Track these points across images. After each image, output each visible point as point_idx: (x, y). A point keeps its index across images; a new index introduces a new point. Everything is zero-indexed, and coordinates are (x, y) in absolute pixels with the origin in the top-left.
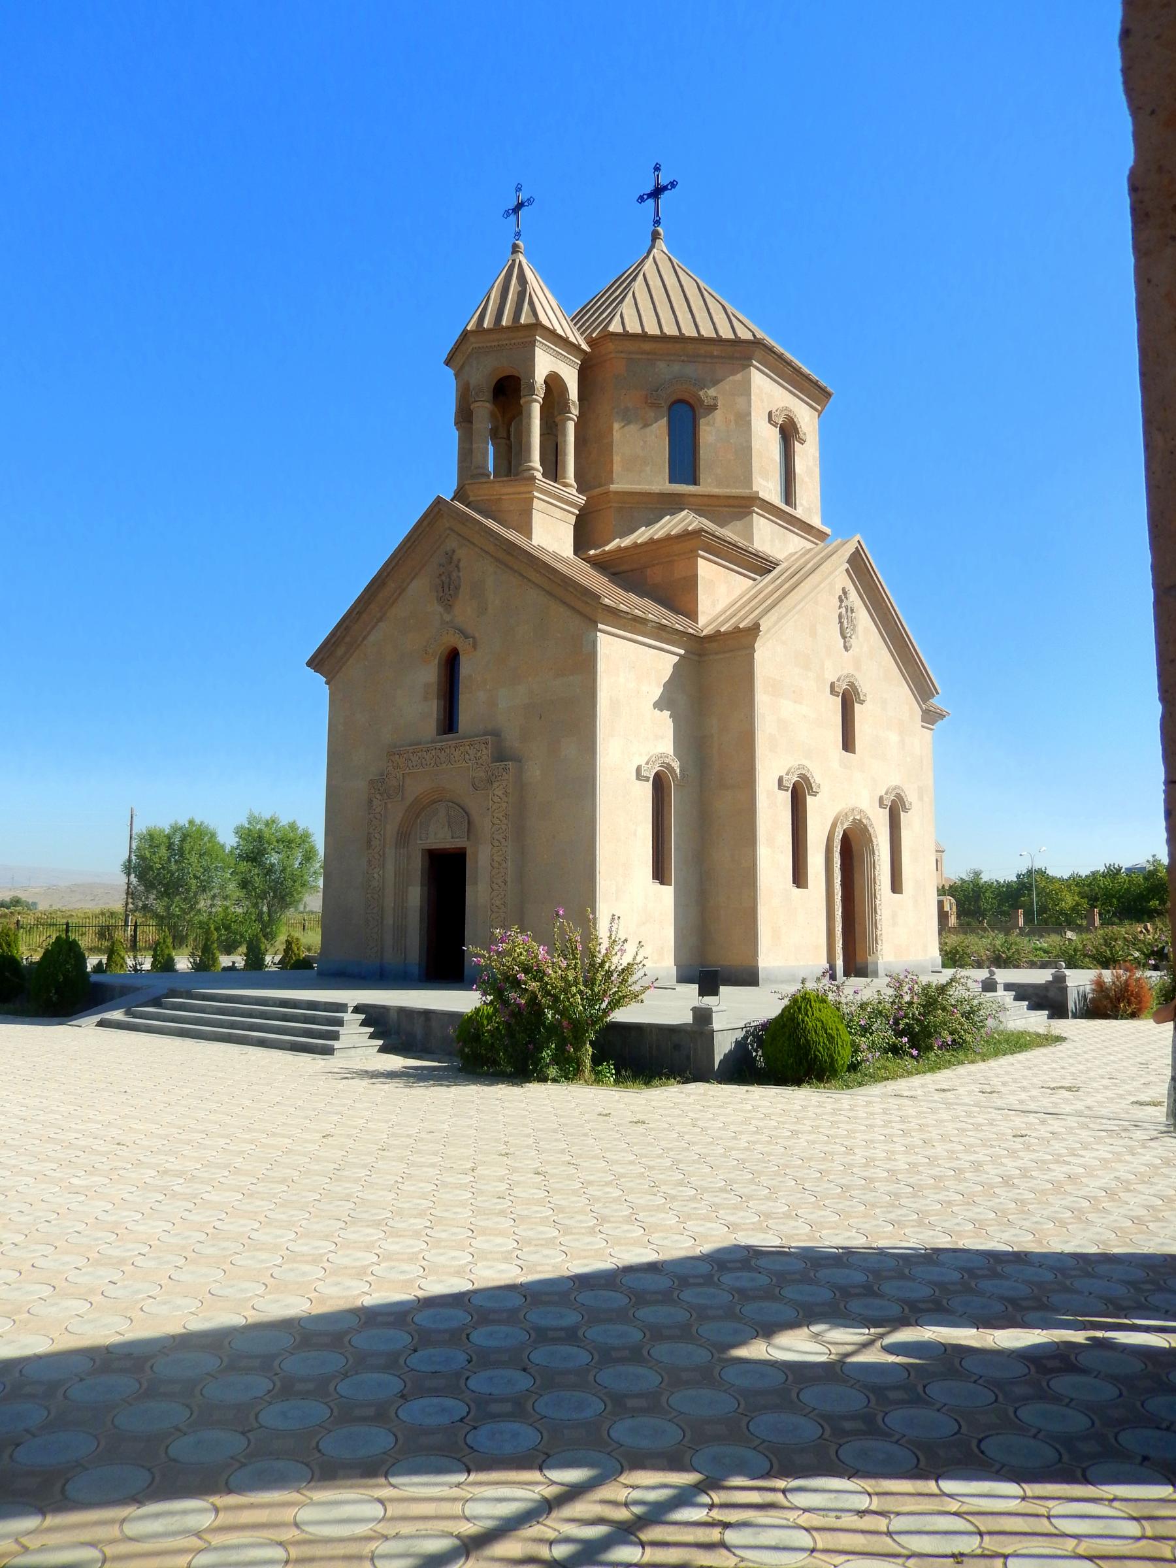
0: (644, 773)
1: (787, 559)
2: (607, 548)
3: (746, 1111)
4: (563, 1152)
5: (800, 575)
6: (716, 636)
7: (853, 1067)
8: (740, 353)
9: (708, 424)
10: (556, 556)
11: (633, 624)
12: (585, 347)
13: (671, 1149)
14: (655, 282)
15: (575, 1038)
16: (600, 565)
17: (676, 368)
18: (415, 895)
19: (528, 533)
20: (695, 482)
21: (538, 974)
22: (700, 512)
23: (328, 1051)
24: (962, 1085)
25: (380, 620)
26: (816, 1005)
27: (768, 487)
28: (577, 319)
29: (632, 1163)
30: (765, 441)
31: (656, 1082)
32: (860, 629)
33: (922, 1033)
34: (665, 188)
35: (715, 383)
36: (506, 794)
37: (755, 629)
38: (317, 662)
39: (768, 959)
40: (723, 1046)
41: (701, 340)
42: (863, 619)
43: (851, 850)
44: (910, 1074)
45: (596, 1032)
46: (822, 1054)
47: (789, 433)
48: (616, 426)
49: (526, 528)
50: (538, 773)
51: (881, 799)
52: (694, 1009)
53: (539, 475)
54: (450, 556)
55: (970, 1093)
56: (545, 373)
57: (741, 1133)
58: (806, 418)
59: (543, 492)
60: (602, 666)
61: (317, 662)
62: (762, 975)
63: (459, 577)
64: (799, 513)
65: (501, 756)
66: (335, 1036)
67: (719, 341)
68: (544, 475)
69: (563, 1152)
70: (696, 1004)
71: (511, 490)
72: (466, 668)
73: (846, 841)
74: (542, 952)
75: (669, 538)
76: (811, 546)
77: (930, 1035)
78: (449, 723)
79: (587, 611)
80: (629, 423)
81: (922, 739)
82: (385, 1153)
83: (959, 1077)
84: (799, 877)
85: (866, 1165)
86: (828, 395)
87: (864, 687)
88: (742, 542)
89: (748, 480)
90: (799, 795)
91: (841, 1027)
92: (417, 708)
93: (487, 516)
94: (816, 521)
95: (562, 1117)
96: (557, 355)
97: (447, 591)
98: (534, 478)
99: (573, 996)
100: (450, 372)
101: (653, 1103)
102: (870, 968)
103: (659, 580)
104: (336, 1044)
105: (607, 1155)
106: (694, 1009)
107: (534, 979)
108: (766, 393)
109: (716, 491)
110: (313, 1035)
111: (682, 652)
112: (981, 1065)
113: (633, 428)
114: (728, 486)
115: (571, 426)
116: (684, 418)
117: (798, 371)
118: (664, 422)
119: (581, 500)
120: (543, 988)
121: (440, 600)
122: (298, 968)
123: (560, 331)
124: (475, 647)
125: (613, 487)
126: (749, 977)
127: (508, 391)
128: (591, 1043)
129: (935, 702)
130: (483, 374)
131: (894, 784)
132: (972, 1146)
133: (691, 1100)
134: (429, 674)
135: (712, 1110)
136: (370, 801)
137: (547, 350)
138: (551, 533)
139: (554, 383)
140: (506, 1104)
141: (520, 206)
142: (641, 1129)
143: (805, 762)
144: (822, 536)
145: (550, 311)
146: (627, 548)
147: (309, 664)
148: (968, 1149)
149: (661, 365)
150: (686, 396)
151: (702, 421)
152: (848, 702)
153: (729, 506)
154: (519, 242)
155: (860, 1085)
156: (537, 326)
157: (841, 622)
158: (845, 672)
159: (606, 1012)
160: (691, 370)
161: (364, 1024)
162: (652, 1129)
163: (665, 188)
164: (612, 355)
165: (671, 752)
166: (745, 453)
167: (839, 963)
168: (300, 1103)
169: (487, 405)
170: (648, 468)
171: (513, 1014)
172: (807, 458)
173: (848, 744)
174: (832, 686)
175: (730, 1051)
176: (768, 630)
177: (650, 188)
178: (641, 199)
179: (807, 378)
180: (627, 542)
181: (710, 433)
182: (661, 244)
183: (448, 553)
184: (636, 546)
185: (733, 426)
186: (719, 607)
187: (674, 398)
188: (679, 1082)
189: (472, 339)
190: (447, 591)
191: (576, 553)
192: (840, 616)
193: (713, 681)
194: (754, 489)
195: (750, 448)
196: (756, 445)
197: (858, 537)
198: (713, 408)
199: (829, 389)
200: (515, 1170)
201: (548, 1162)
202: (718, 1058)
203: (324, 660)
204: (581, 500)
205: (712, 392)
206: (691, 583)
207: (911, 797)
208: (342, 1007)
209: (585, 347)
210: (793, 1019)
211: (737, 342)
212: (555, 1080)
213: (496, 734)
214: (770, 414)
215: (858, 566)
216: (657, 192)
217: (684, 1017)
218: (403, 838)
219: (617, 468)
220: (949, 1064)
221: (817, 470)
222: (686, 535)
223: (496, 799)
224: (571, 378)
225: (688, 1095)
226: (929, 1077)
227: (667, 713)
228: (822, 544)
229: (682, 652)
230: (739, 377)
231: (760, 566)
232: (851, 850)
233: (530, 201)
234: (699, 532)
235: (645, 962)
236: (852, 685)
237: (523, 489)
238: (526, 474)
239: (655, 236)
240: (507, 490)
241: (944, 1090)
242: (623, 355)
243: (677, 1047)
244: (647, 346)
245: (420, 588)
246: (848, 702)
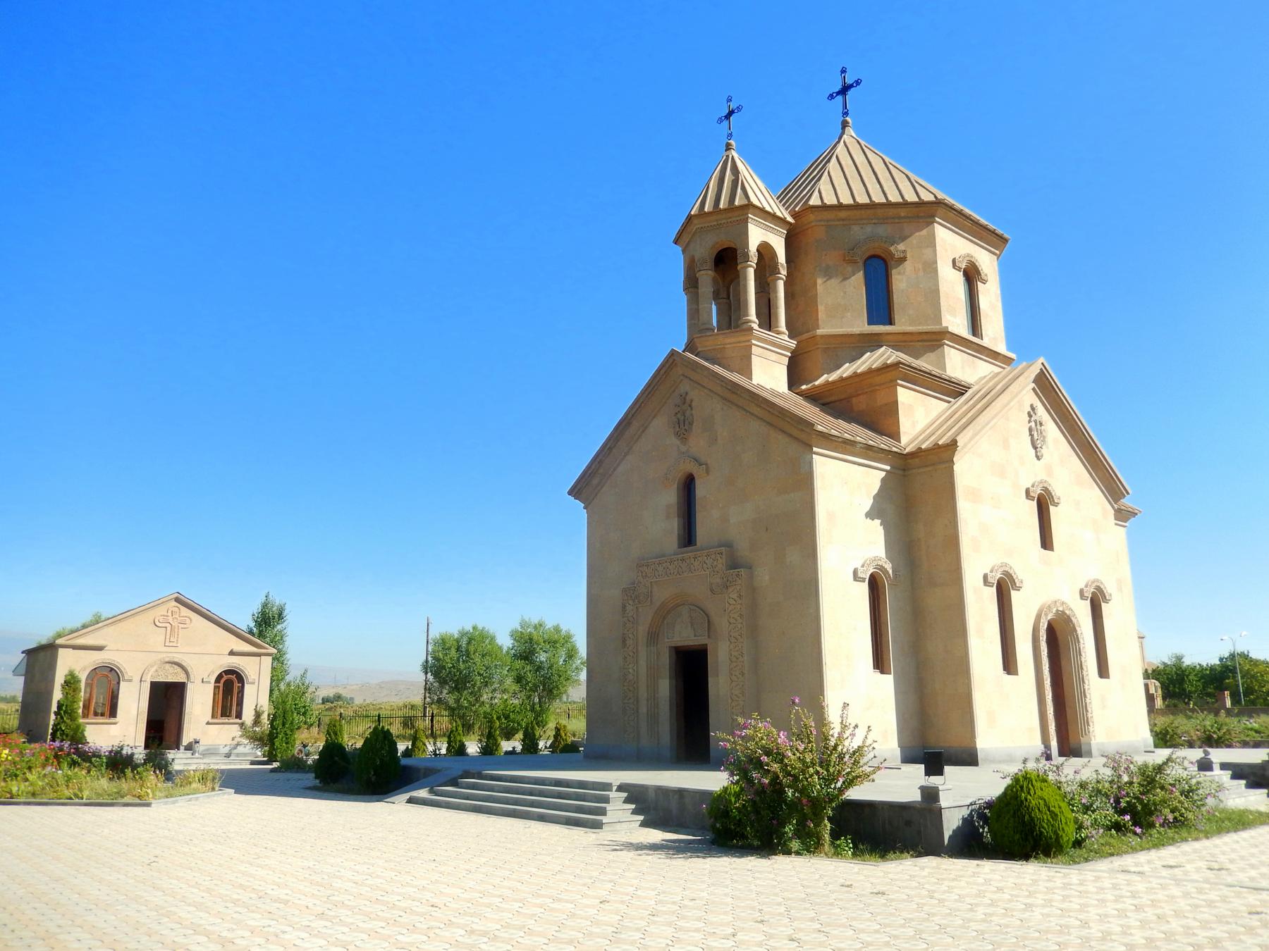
0: (860, 575)
1: (977, 383)
2: (817, 383)
3: (978, 884)
4: (812, 920)
5: (990, 397)
6: (918, 453)
7: (1078, 844)
8: (923, 213)
10: (773, 392)
11: (844, 446)
12: (790, 219)
13: (912, 920)
14: (846, 161)
15: (814, 814)
16: (812, 397)
17: (869, 229)
18: (665, 687)
19: (749, 375)
20: (891, 323)
21: (780, 757)
22: (896, 347)
23: (597, 825)
24: (1189, 862)
26: (1038, 785)
27: (956, 322)
28: (781, 198)
29: (877, 932)
30: (951, 284)
31: (891, 855)
32: (1050, 439)
33: (1142, 812)
34: (851, 86)
35: (903, 239)
36: (740, 597)
37: (953, 445)
38: (576, 492)
39: (985, 741)
40: (951, 822)
41: (889, 205)
42: (1052, 431)
43: (1057, 638)
44: (1134, 850)
45: (833, 809)
46: (1047, 830)
47: (971, 276)
48: (819, 281)
49: (747, 372)
50: (767, 578)
51: (1081, 592)
52: (923, 789)
53: (755, 326)
54: (683, 397)
55: (1198, 870)
57: (977, 905)
58: (987, 261)
59: (759, 339)
61: (576, 492)
62: (980, 756)
64: (986, 342)
65: (734, 564)
66: (603, 812)
67: (905, 204)
68: (760, 326)
69: (812, 920)
70: (923, 784)
71: (733, 340)
72: (700, 491)
73: (1051, 630)
74: (782, 738)
75: (870, 372)
76: (999, 370)
77: (1151, 813)
78: (688, 537)
79: (804, 438)
80: (830, 278)
81: (1117, 535)
82: (655, 918)
83: (1184, 854)
84: (1009, 665)
85: (1103, 939)
86: (1005, 241)
87: (1057, 490)
88: (936, 371)
89: (938, 317)
90: (1004, 590)
91: (1063, 805)
92: (660, 524)
93: (713, 363)
94: (1001, 348)
95: (808, 887)
96: (767, 228)
97: (682, 426)
98: (752, 329)
99: (811, 776)
100: (678, 249)
101: (891, 876)
102: (1084, 748)
103: (863, 407)
104: (605, 819)
105: (854, 923)
106: (923, 789)
107: (775, 760)
108: (949, 244)
110: (583, 812)
111: (888, 468)
112: (1205, 843)
113: (834, 282)
114: (920, 324)
115: (781, 285)
116: (878, 272)
117: (976, 223)
118: (861, 275)
119: (793, 344)
120: (782, 770)
121: (677, 434)
122: (565, 751)
123: (768, 209)
124: (708, 472)
125: (819, 332)
126: (969, 758)
127: (727, 260)
128: (830, 819)
129: (1126, 502)
130: (705, 248)
131: (1092, 578)
132: (1208, 922)
133: (925, 873)
134: (670, 497)
135: (946, 883)
136: (624, 607)
137: (758, 225)
138: (768, 373)
139: (765, 251)
140: (757, 875)
141: (731, 113)
142: (882, 900)
144: (1007, 360)
145: (759, 193)
146: (834, 382)
147: (570, 493)
148: (1205, 925)
149: (856, 228)
150: (879, 252)
151: (894, 272)
152: (1044, 505)
154: (732, 142)
155: (1087, 860)
156: (749, 206)
157: (1031, 435)
158: (1039, 479)
159: (841, 791)
160: (882, 230)
161: (627, 801)
162: (892, 900)
163: (851, 86)
165: (883, 555)
166: (933, 295)
167: (1054, 744)
168: (578, 871)
171: (758, 793)
172: (990, 296)
173: (1046, 541)
174: (1027, 491)
175: (958, 828)
176: (965, 445)
177: (838, 87)
178: (831, 97)
179: (985, 228)
180: (833, 377)
181: (901, 281)
182: (850, 131)
183: (681, 395)
184: (842, 379)
185: (921, 273)
186: (919, 427)
188: (912, 856)
189: (696, 221)
190: (682, 426)
191: (790, 388)
192: (1030, 430)
193: (918, 494)
194: (944, 324)
195: (937, 291)
196: (943, 288)
197: (1042, 360)
198: (903, 260)
199: (1006, 236)
200: (771, 937)
201: (801, 930)
202: (947, 834)
204: (793, 344)
205: (901, 247)
206: (892, 409)
207: (1110, 588)
208: (606, 786)
209: (790, 219)
210: (1016, 797)
211: (921, 204)
212: (798, 853)
213: (729, 545)
214: (954, 261)
215: (1044, 385)
216: (845, 90)
217: (915, 796)
218: (653, 637)
220: (1173, 841)
221: (1000, 305)
222: (886, 368)
223: (732, 602)
225: (922, 868)
226: (1153, 854)
227: (878, 522)
228: (1008, 368)
229: (888, 468)
230: (924, 232)
231: (954, 390)
232: (1057, 638)
234: (897, 364)
235: (875, 745)
236: (1046, 490)
238: (745, 326)
239: (845, 125)
240: (730, 341)
241: (1171, 867)
243: (908, 823)
244: (843, 214)
245: (660, 425)
246: (1044, 505)
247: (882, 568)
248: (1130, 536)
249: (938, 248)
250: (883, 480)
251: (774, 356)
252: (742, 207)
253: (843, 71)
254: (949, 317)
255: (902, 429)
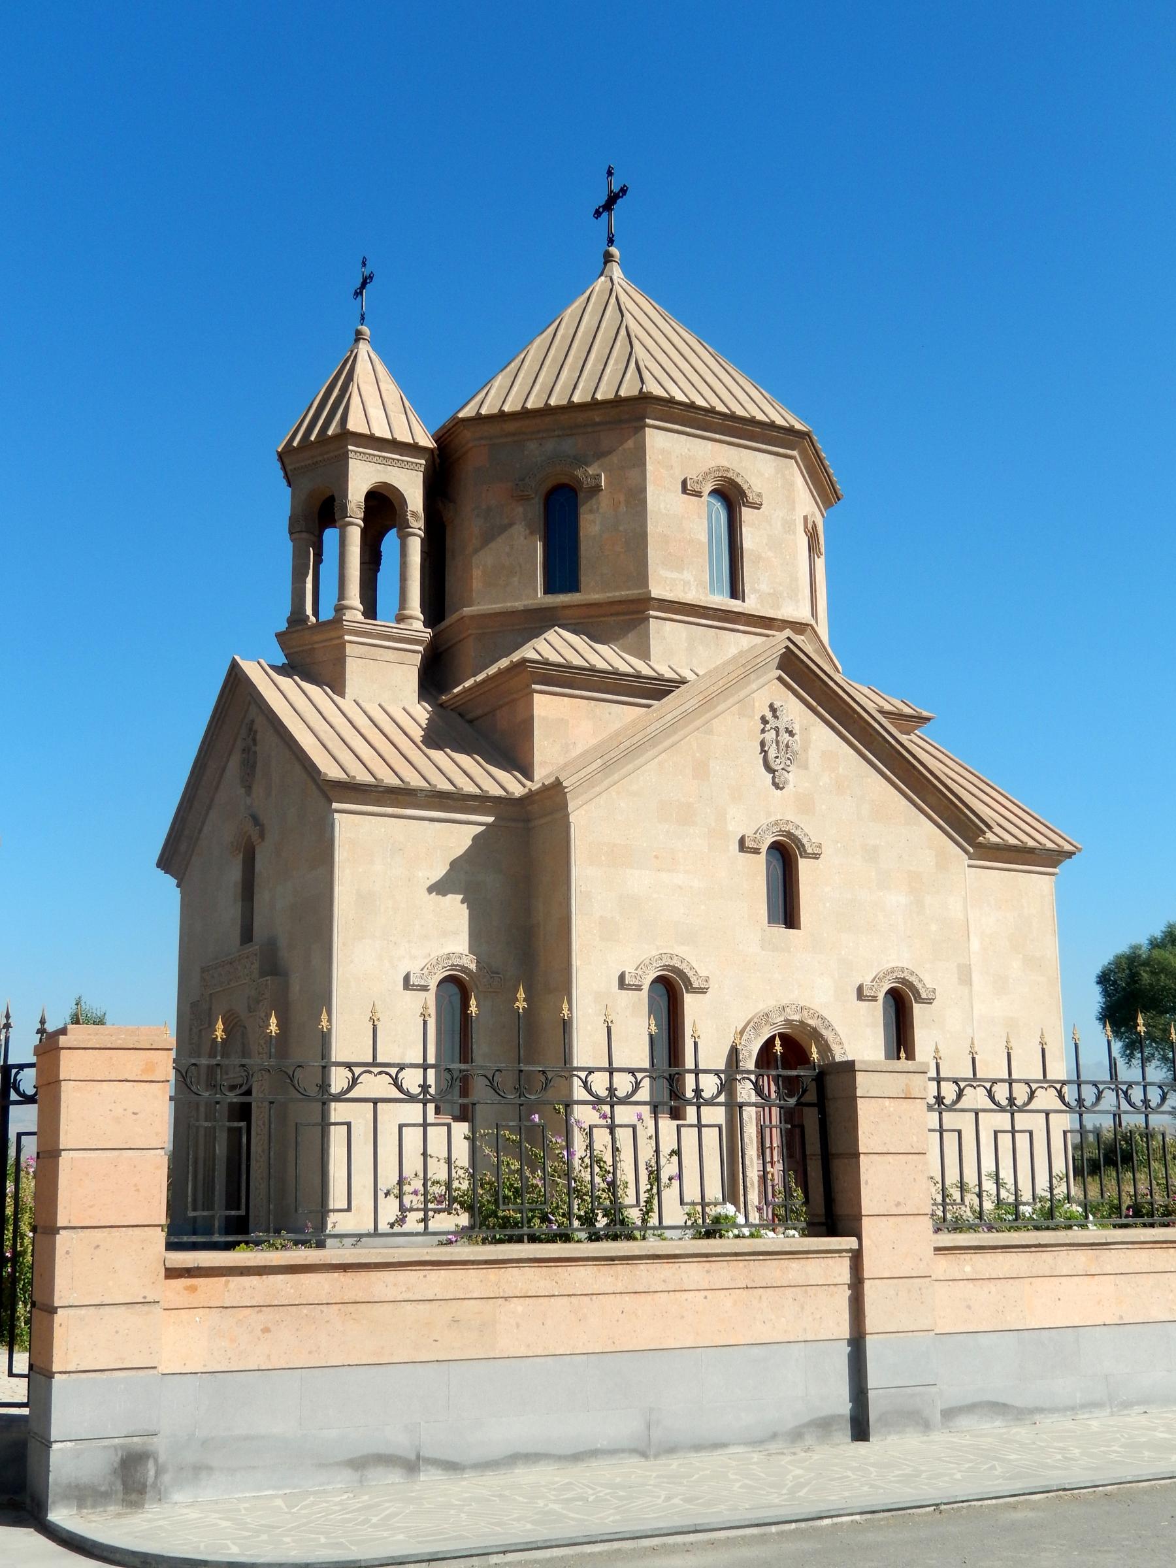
9: (591, 511)
17: (550, 446)
25: (209, 808)
35: (600, 455)
42: (819, 739)
47: (731, 497)
56: (365, 489)
60: (341, 854)
61: (166, 862)
63: (255, 752)
72: (261, 864)
75: (501, 673)
89: (641, 575)
96: (386, 462)
97: (249, 766)
109: (596, 597)
111: (490, 819)
124: (262, 836)
125: (467, 611)
134: (235, 874)
141: (364, 284)
143: (680, 950)
147: (158, 866)
149: (532, 446)
152: (785, 858)
153: (618, 614)
154: (365, 329)
156: (346, 436)
157: (764, 752)
160: (569, 446)
164: (470, 445)
165: (467, 952)
166: (637, 542)
169: (304, 535)
170: (516, 579)
181: (592, 525)
187: (549, 484)
192: (762, 744)
195: (644, 535)
203: (166, 862)
206: (526, 728)
211: (618, 402)
214: (684, 483)
216: (609, 205)
219: (477, 584)
224: (411, 487)
229: (490, 819)
230: (630, 444)
233: (624, 190)
237: (333, 634)
239: (608, 258)
242: (483, 442)
244: (510, 427)
246: (785, 858)
247: (464, 969)
248: (1058, 886)
249: (650, 467)
250: (476, 838)
251: (390, 655)
252: (335, 437)
253: (610, 173)
254: (664, 573)
255: (537, 758)
